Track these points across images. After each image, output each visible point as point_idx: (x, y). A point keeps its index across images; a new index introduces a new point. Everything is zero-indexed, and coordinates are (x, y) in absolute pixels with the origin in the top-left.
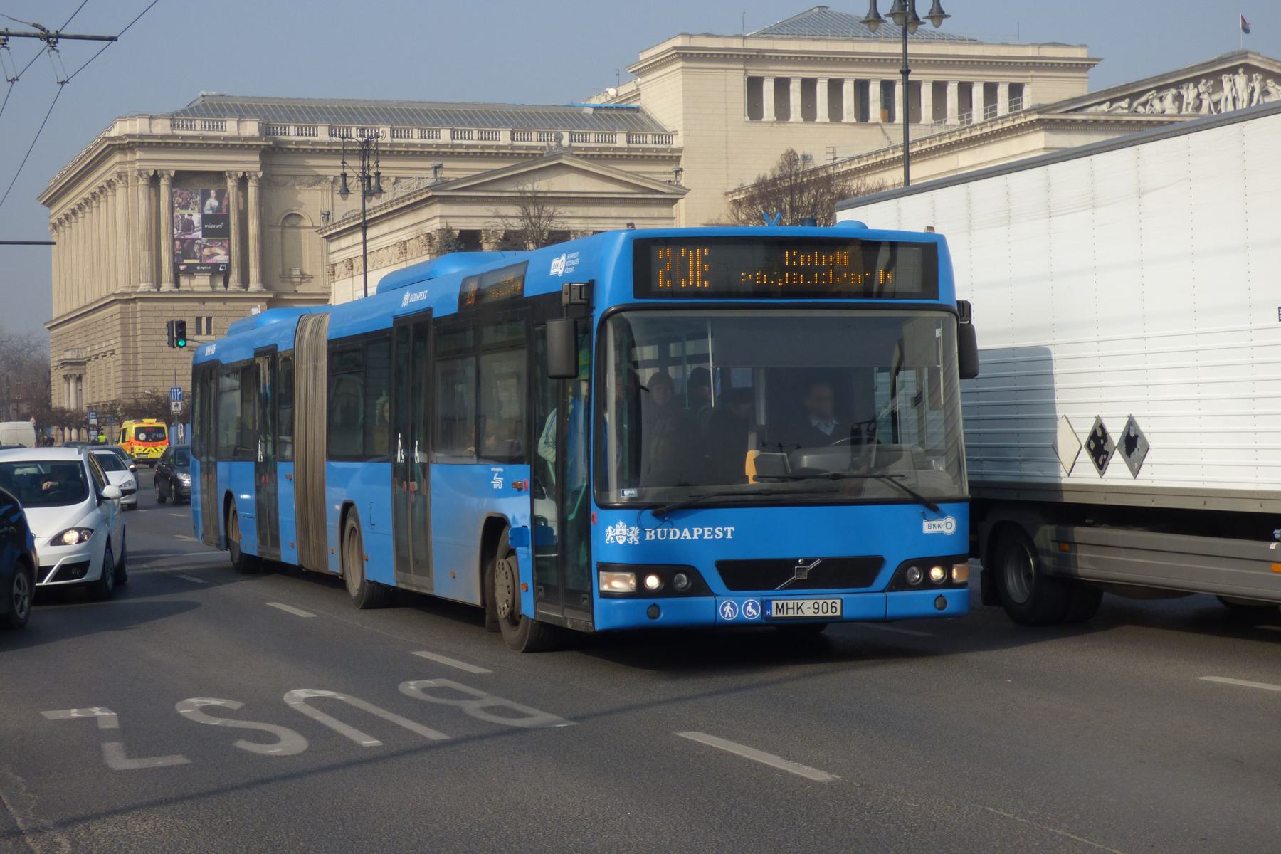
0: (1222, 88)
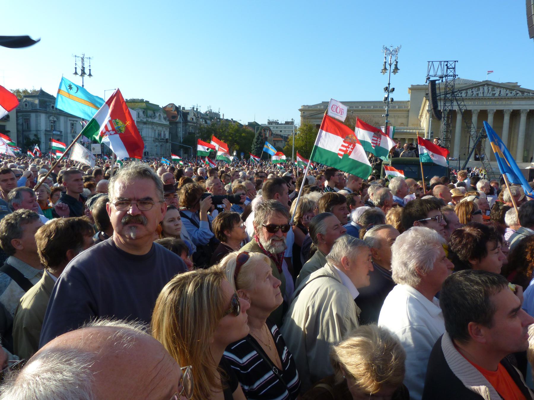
0: (480, 90)
